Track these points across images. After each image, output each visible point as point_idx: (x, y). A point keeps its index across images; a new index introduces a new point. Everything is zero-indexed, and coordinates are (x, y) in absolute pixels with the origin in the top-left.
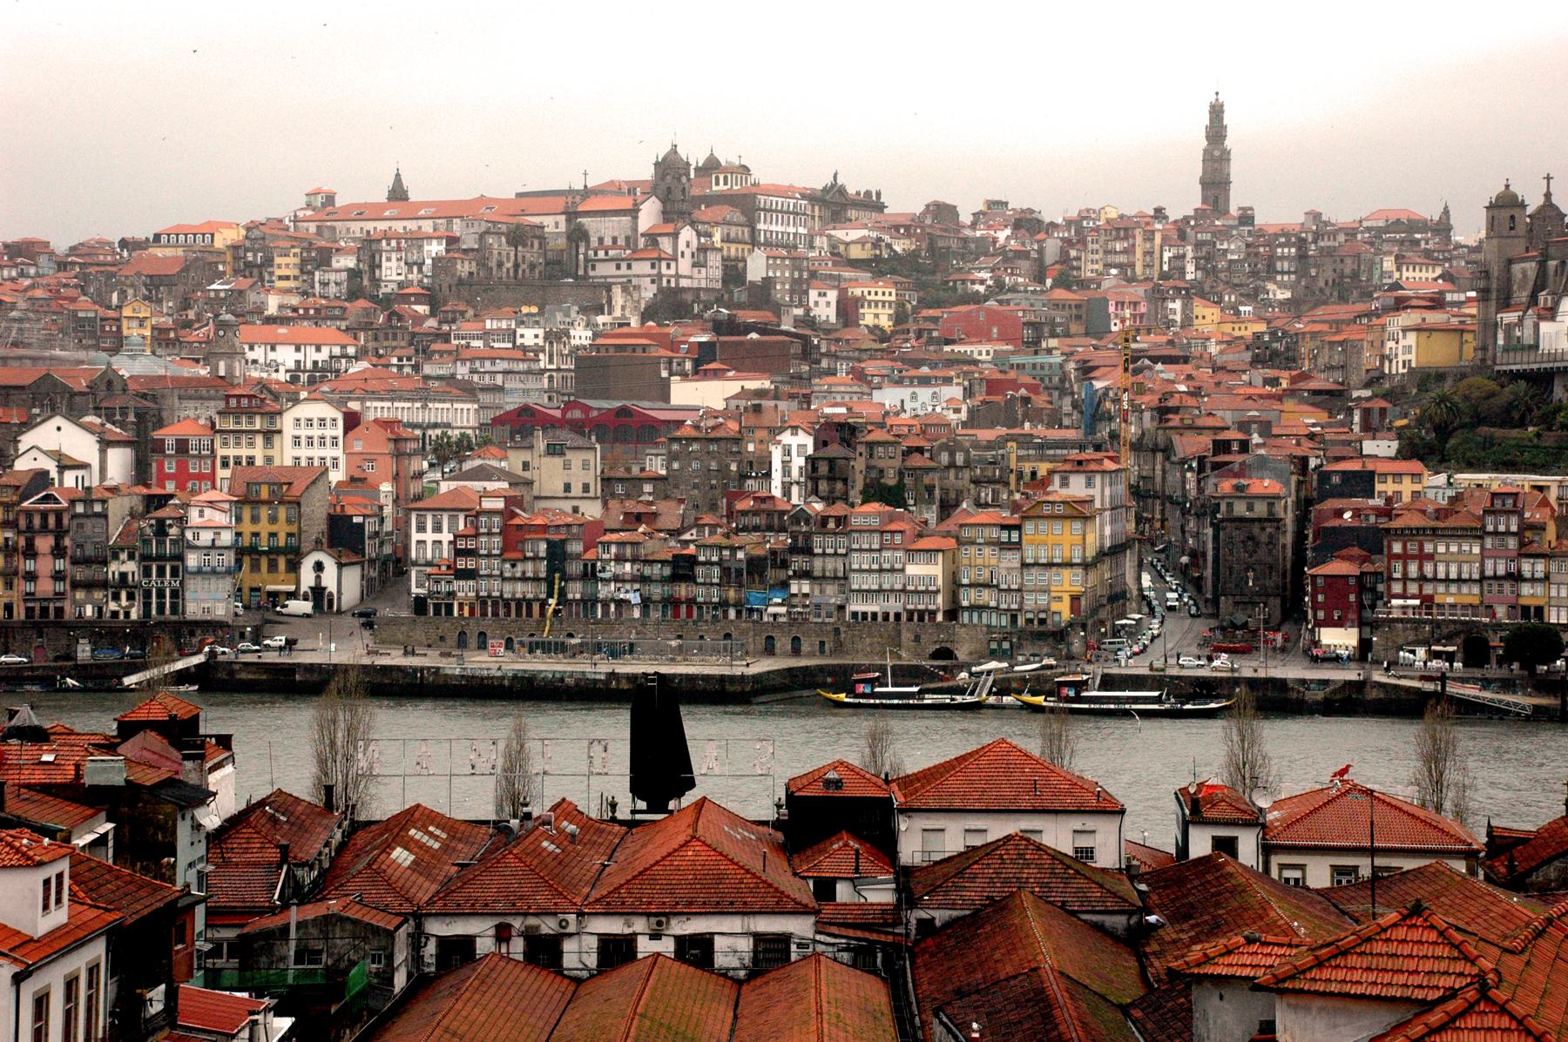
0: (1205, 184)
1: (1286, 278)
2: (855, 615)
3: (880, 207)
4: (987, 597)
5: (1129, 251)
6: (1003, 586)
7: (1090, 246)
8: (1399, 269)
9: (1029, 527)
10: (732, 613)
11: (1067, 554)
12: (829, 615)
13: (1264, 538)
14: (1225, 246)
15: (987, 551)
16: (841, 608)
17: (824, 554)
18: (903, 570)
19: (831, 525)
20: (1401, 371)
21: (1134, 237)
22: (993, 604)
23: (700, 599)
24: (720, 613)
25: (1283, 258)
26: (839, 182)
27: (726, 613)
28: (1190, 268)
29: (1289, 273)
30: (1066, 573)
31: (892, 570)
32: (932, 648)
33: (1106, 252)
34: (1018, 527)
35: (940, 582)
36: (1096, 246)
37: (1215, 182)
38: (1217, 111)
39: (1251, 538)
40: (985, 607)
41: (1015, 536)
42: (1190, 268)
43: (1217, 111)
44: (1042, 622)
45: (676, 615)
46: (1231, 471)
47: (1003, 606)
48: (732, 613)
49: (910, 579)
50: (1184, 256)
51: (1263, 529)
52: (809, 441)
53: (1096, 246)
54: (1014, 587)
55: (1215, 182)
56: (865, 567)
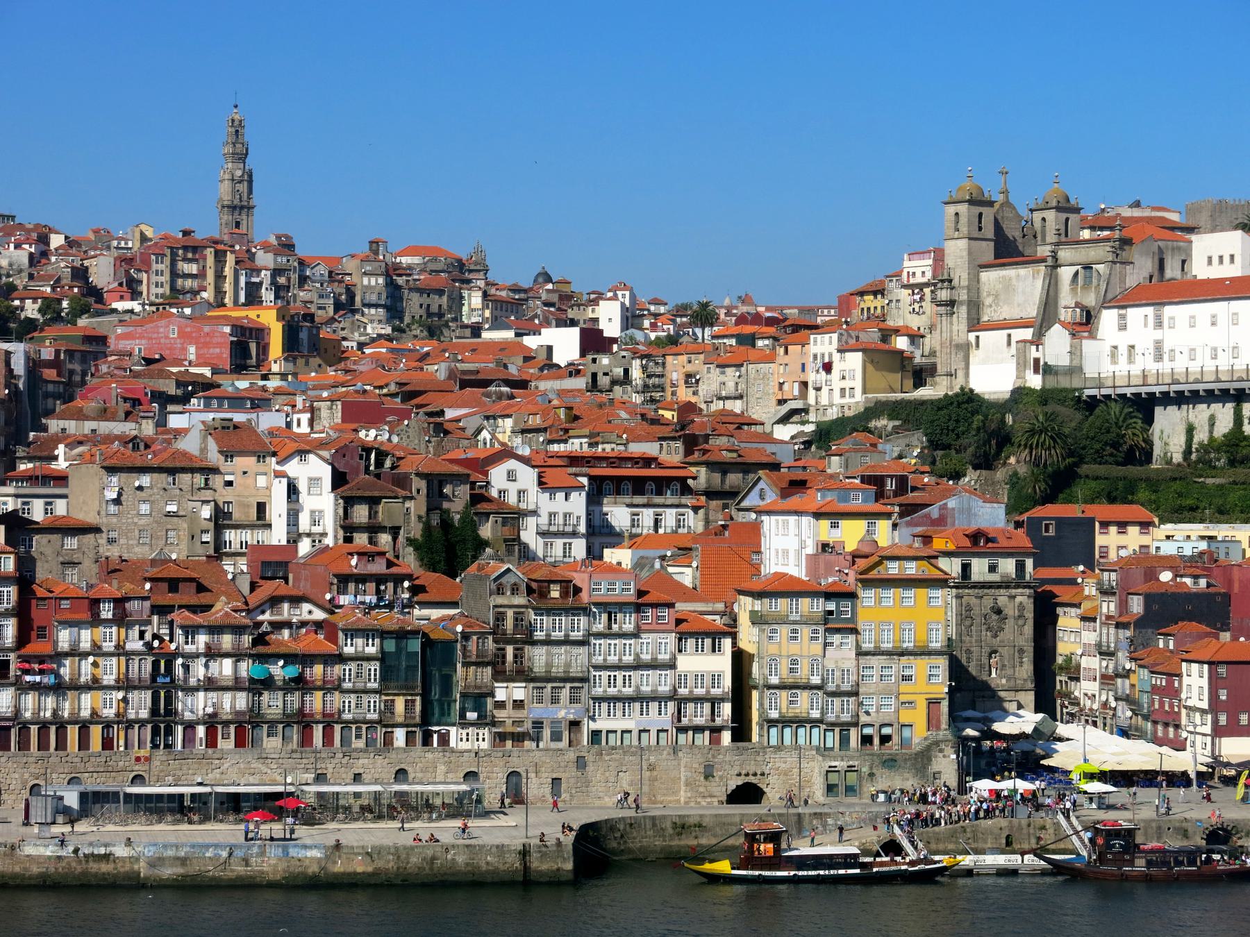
2: (595, 735)
4: (804, 704)
5: (201, 275)
6: (831, 687)
7: (155, 267)
9: (868, 597)
10: (400, 735)
11: (922, 637)
12: (556, 737)
13: (1010, 610)
15: (805, 631)
16: (575, 724)
17: (548, 642)
18: (672, 665)
19: (555, 593)
20: (837, 400)
21: (205, 259)
22: (815, 714)
23: (347, 716)
24: (380, 732)
27: (388, 741)
30: (919, 667)
31: (654, 665)
32: (734, 783)
34: (852, 596)
35: (727, 682)
36: (160, 267)
38: (237, 130)
39: (999, 611)
40: (800, 722)
41: (846, 606)
43: (237, 130)
44: (885, 739)
45: (306, 740)
46: (928, 516)
47: (831, 717)
48: (400, 735)
49: (681, 679)
51: (1013, 597)
52: (325, 472)
53: (160, 267)
54: (846, 687)
56: (613, 659)
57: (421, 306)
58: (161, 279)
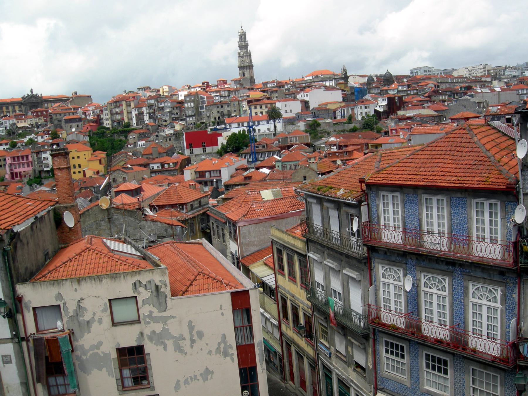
0: (240, 68)
1: (191, 119)
3: (150, 88)
8: (250, 109)
14: (163, 105)
21: (122, 105)
25: (188, 108)
26: (34, 93)
28: (146, 119)
29: (192, 116)
33: (112, 114)
36: (107, 112)
37: (246, 66)
38: (243, 37)
42: (146, 119)
43: (243, 37)
50: (143, 113)
53: (107, 112)
55: (246, 66)
57: (219, 112)
58: (107, 117)
